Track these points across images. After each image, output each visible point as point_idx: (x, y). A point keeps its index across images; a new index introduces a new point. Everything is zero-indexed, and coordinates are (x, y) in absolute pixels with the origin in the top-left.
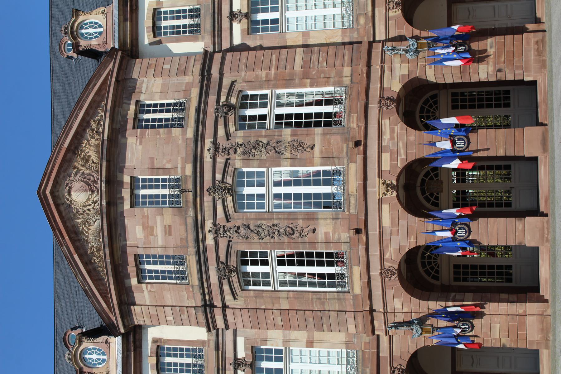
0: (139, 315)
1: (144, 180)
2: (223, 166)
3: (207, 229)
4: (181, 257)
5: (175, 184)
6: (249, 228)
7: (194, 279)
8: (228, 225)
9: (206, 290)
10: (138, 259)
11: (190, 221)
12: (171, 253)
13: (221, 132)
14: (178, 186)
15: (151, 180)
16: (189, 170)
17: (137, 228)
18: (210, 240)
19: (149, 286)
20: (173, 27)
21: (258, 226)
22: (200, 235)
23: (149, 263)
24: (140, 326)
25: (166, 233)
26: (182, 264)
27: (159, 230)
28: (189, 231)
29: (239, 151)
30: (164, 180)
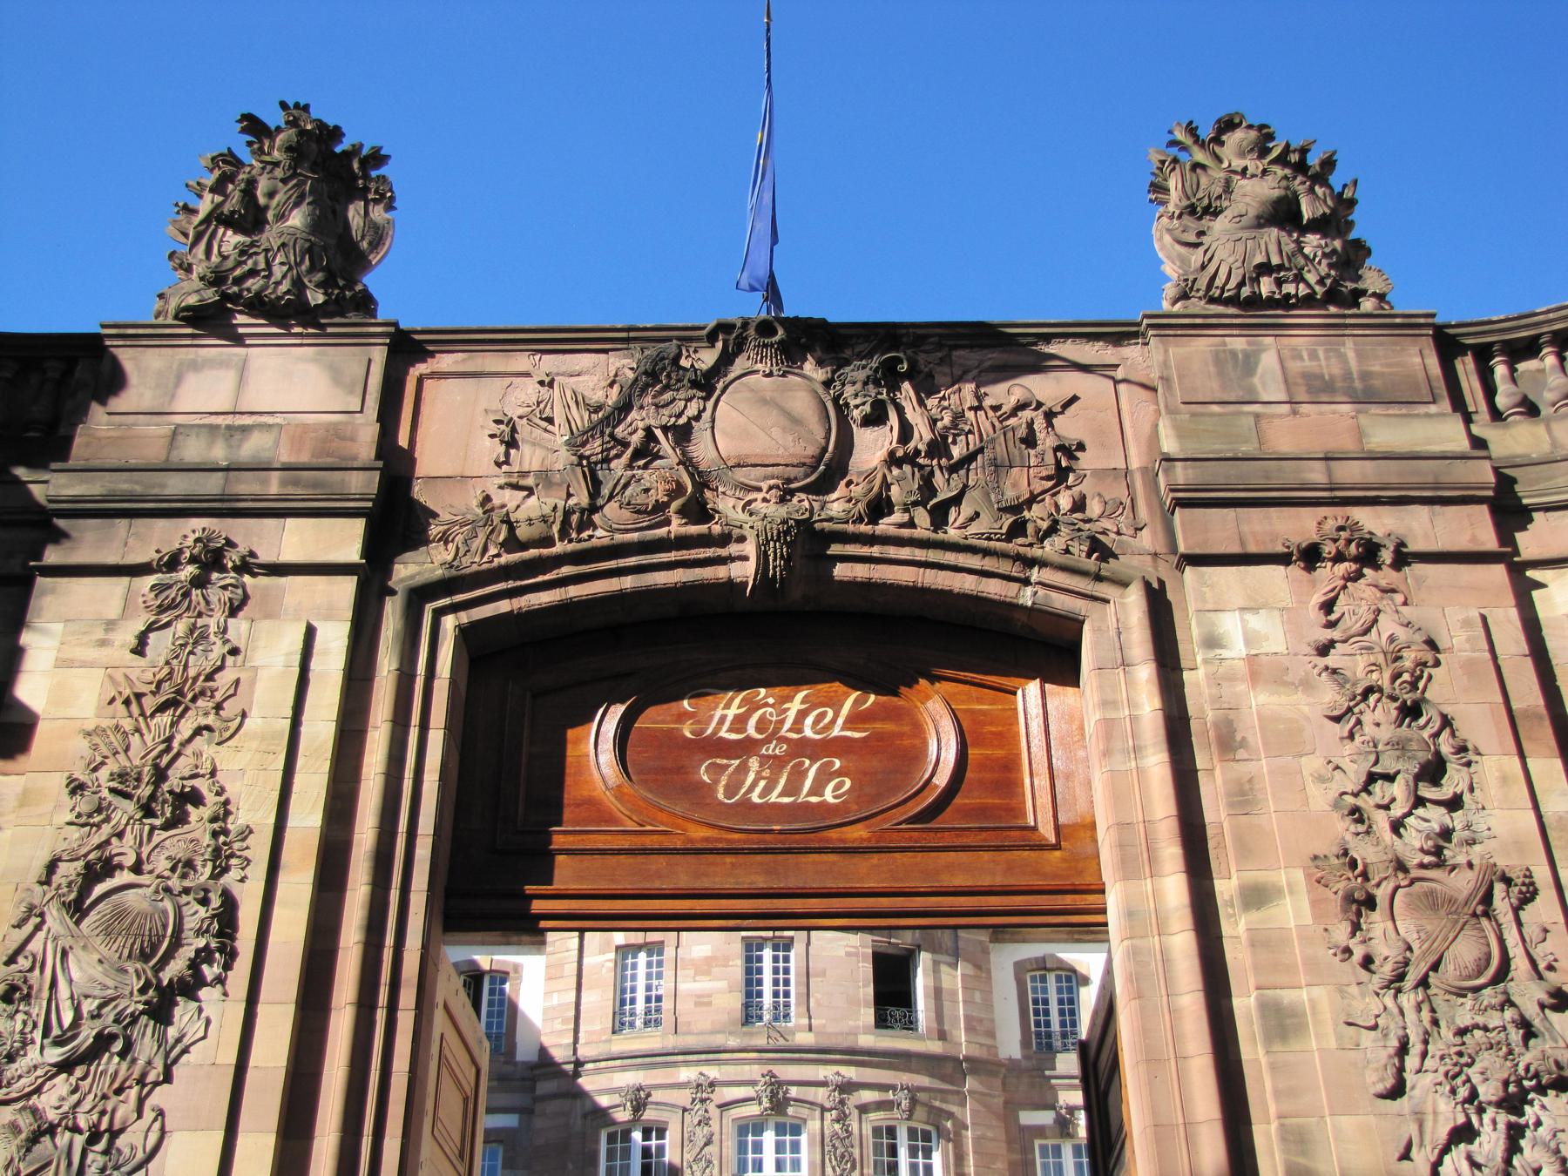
0: (562, 943)
1: (786, 959)
2: (811, 1099)
3: (706, 1069)
4: (658, 1023)
5: (781, 1013)
6: (706, 1144)
7: (622, 1044)
8: (711, 1107)
9: (603, 1064)
10: (655, 949)
11: (719, 1040)
12: (667, 1004)
13: (867, 1096)
14: (776, 1019)
15: (787, 971)
16: (804, 1039)
17: (709, 947)
18: (687, 1074)
19: (612, 965)
20: (1046, 1002)
21: (710, 1162)
22: (695, 1057)
23: (649, 965)
24: (544, 943)
25: (698, 996)
26: (647, 1023)
27: (704, 985)
28: (701, 1038)
29: (837, 1126)
30: (787, 994)
